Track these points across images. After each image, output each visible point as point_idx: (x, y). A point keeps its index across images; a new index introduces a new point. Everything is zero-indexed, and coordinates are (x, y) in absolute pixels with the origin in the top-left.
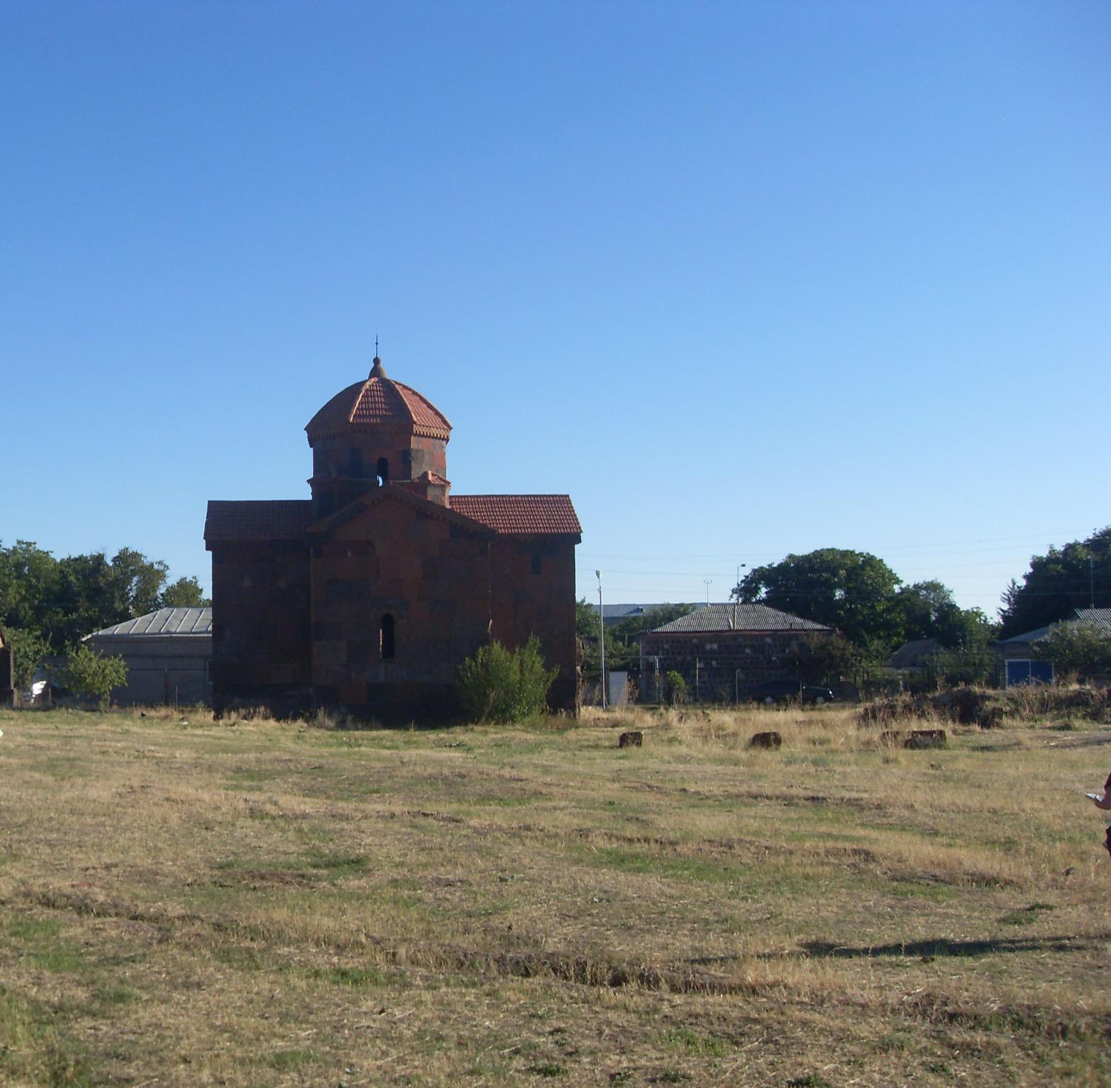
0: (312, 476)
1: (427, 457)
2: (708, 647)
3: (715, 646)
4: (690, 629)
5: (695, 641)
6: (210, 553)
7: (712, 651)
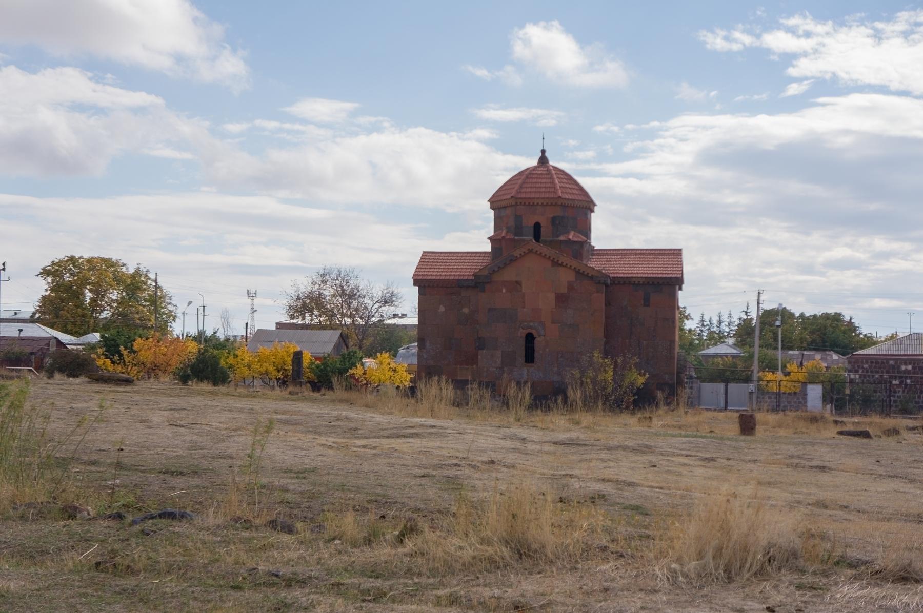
0: (492, 234)
2: (903, 367)
3: (910, 367)
4: (890, 353)
5: (892, 362)
7: (906, 371)
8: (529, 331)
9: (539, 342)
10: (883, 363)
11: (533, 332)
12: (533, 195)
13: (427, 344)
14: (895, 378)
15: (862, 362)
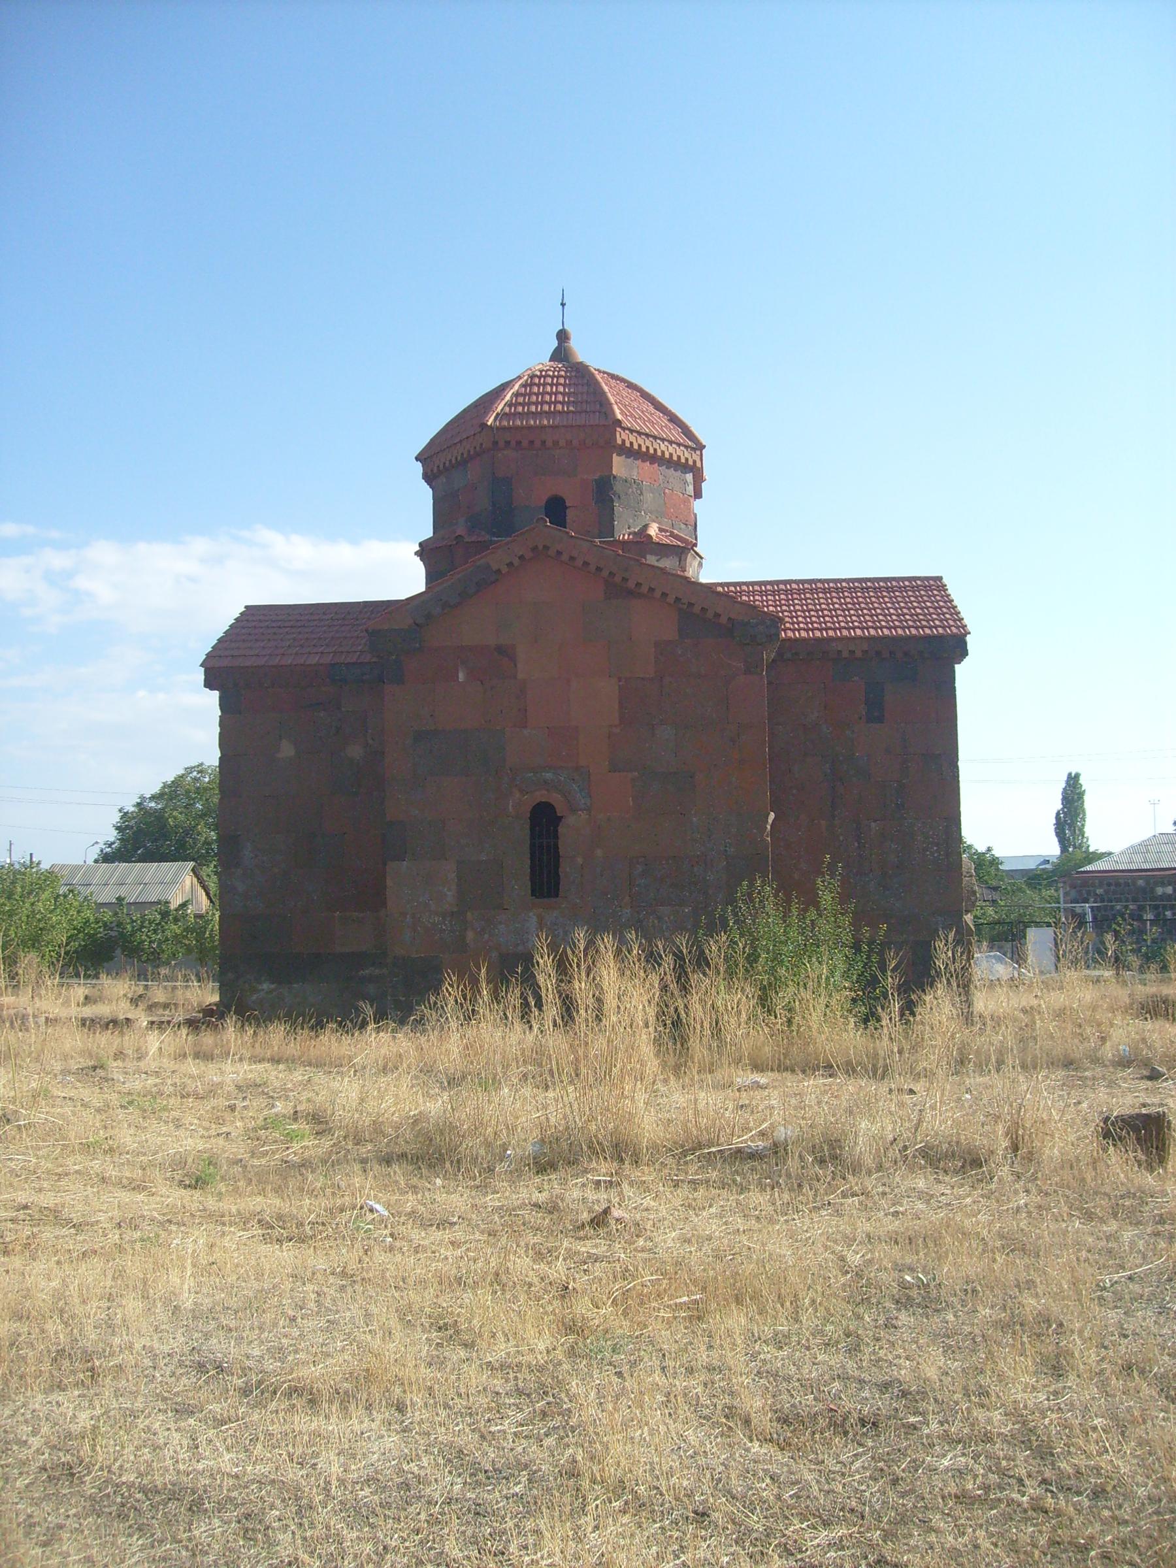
1: (648, 496)
2: (1160, 891)
5: (1141, 882)
6: (216, 694)
8: (541, 796)
9: (573, 830)
10: (1127, 884)
11: (556, 799)
15: (1093, 885)
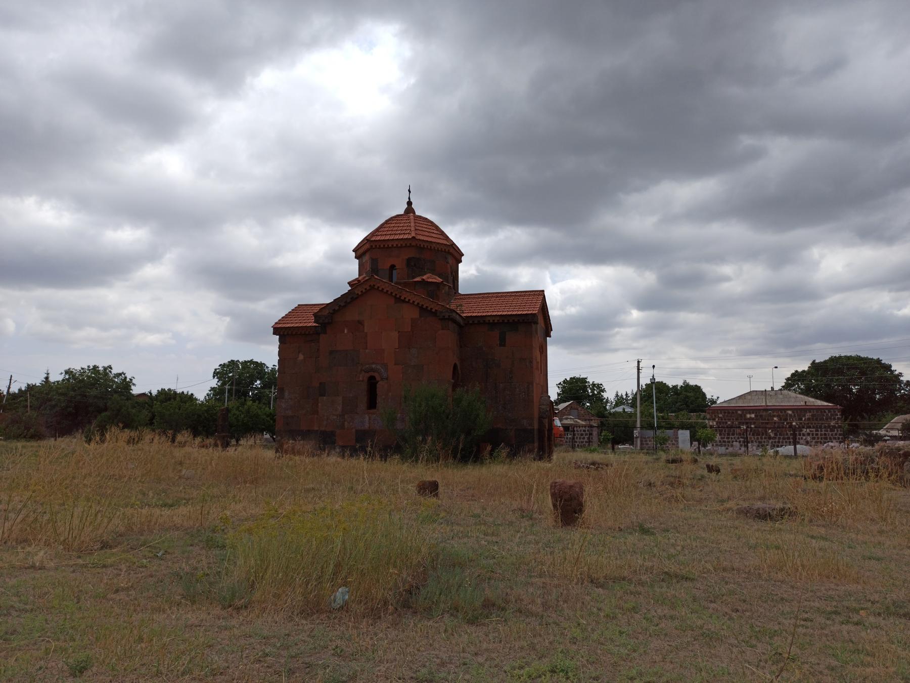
2: (748, 416)
3: (753, 416)
8: (372, 374)
9: (381, 386)
11: (376, 375)
12: (387, 238)
13: (286, 394)
14: (743, 424)
